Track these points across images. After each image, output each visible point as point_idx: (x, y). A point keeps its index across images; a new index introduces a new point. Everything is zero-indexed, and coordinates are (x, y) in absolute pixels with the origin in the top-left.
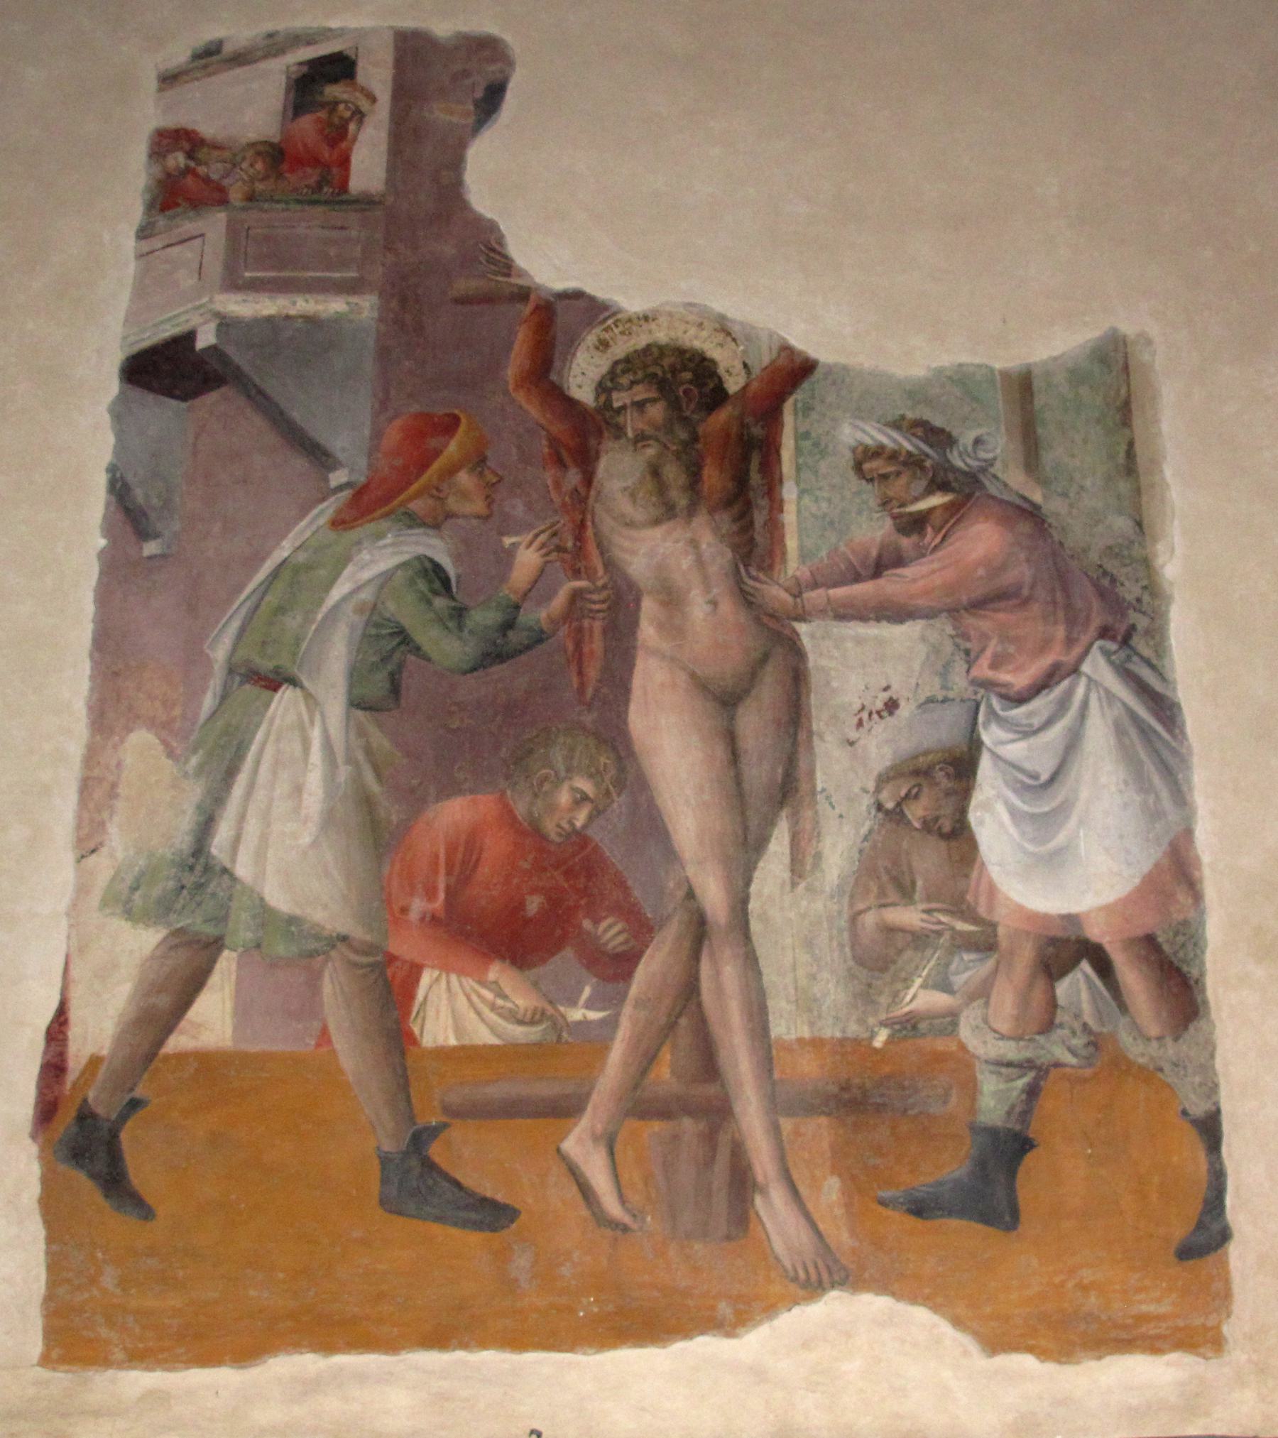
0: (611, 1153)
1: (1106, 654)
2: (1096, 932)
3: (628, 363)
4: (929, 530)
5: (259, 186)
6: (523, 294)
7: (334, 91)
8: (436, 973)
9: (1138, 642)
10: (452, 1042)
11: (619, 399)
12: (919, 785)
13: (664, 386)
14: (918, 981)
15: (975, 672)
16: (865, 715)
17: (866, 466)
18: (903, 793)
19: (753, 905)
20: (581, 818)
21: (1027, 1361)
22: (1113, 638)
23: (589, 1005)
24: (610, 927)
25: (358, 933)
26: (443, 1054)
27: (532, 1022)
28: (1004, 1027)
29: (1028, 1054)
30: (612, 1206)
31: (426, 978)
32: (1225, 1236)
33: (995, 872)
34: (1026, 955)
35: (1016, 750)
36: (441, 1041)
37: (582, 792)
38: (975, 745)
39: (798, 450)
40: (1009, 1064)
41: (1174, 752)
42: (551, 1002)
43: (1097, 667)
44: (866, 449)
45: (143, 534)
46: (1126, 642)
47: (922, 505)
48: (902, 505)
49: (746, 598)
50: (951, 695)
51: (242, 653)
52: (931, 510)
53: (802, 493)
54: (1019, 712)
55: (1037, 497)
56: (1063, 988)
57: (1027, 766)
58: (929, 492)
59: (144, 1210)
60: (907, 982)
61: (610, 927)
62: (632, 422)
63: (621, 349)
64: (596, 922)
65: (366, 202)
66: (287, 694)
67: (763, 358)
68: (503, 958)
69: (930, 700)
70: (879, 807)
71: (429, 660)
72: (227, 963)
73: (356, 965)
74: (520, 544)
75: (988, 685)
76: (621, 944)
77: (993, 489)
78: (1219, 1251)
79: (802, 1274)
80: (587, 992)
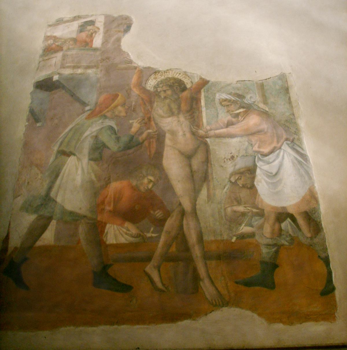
0: (159, 271)
1: (288, 144)
2: (291, 211)
3: (162, 82)
4: (240, 117)
5: (71, 47)
6: (135, 68)
7: (89, 28)
8: (110, 225)
9: (296, 141)
10: (115, 242)
11: (159, 90)
12: (241, 176)
13: (171, 87)
14: (243, 225)
15: (254, 149)
16: (226, 160)
17: (223, 103)
18: (237, 178)
19: (197, 207)
20: (150, 186)
21: (281, 326)
22: (289, 140)
23: (153, 233)
24: (159, 212)
25: (89, 215)
26: (112, 245)
27: (137, 237)
28: (268, 235)
29: (275, 242)
30: (160, 285)
31: (108, 226)
32: (333, 289)
33: (262, 197)
34: (272, 218)
35: (266, 167)
36: (111, 242)
37: (151, 180)
38: (255, 166)
39: (206, 101)
40: (270, 245)
41: (308, 167)
42: (142, 232)
43: (285, 147)
44: (223, 99)
45: (37, 120)
46: (292, 141)
47: (238, 111)
48: (233, 111)
49: (193, 134)
50: (248, 154)
51: (61, 149)
52: (240, 113)
53: (207, 109)
54: (266, 158)
55: (267, 109)
56: (283, 225)
57: (270, 171)
58: (239, 108)
59: (27, 288)
60: (240, 224)
61: (159, 212)
62: (163, 95)
63: (160, 78)
64: (155, 211)
65: (96, 50)
66: (72, 159)
67: (196, 80)
68: (129, 221)
69: (243, 156)
70: (231, 182)
71: (110, 149)
72: (54, 223)
73: (88, 223)
74: (134, 122)
75: (258, 152)
76: (161, 217)
77: (255, 107)
78: (332, 293)
79: (214, 303)
80: (152, 229)
